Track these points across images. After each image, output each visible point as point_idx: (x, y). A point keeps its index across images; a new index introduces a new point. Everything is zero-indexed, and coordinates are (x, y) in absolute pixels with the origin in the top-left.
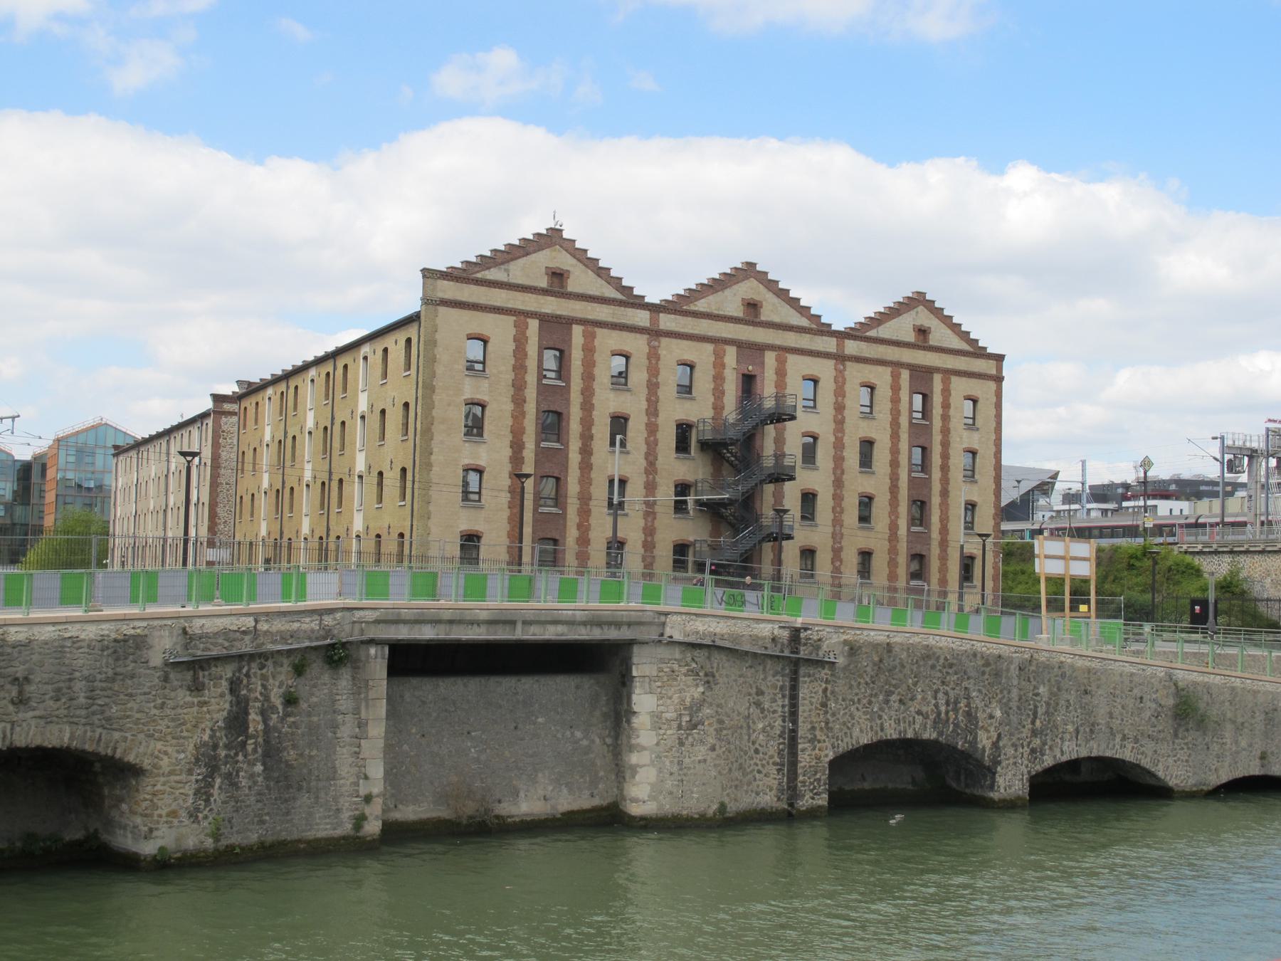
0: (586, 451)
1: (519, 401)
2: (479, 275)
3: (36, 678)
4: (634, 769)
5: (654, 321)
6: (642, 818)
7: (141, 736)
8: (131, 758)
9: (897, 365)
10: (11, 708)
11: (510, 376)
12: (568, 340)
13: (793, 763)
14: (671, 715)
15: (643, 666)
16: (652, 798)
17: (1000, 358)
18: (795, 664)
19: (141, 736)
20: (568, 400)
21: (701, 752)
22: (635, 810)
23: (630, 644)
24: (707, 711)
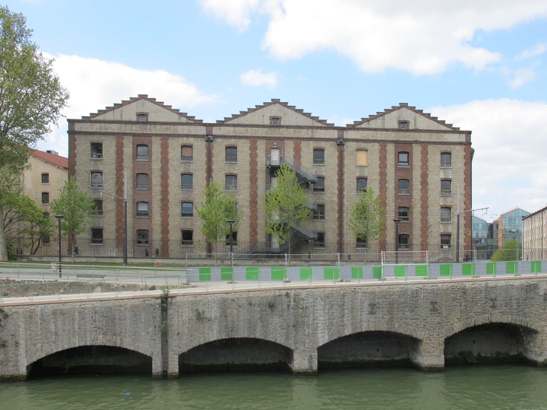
3: (498, 299)
7: (537, 320)
8: (533, 327)
10: (490, 309)
19: (537, 320)
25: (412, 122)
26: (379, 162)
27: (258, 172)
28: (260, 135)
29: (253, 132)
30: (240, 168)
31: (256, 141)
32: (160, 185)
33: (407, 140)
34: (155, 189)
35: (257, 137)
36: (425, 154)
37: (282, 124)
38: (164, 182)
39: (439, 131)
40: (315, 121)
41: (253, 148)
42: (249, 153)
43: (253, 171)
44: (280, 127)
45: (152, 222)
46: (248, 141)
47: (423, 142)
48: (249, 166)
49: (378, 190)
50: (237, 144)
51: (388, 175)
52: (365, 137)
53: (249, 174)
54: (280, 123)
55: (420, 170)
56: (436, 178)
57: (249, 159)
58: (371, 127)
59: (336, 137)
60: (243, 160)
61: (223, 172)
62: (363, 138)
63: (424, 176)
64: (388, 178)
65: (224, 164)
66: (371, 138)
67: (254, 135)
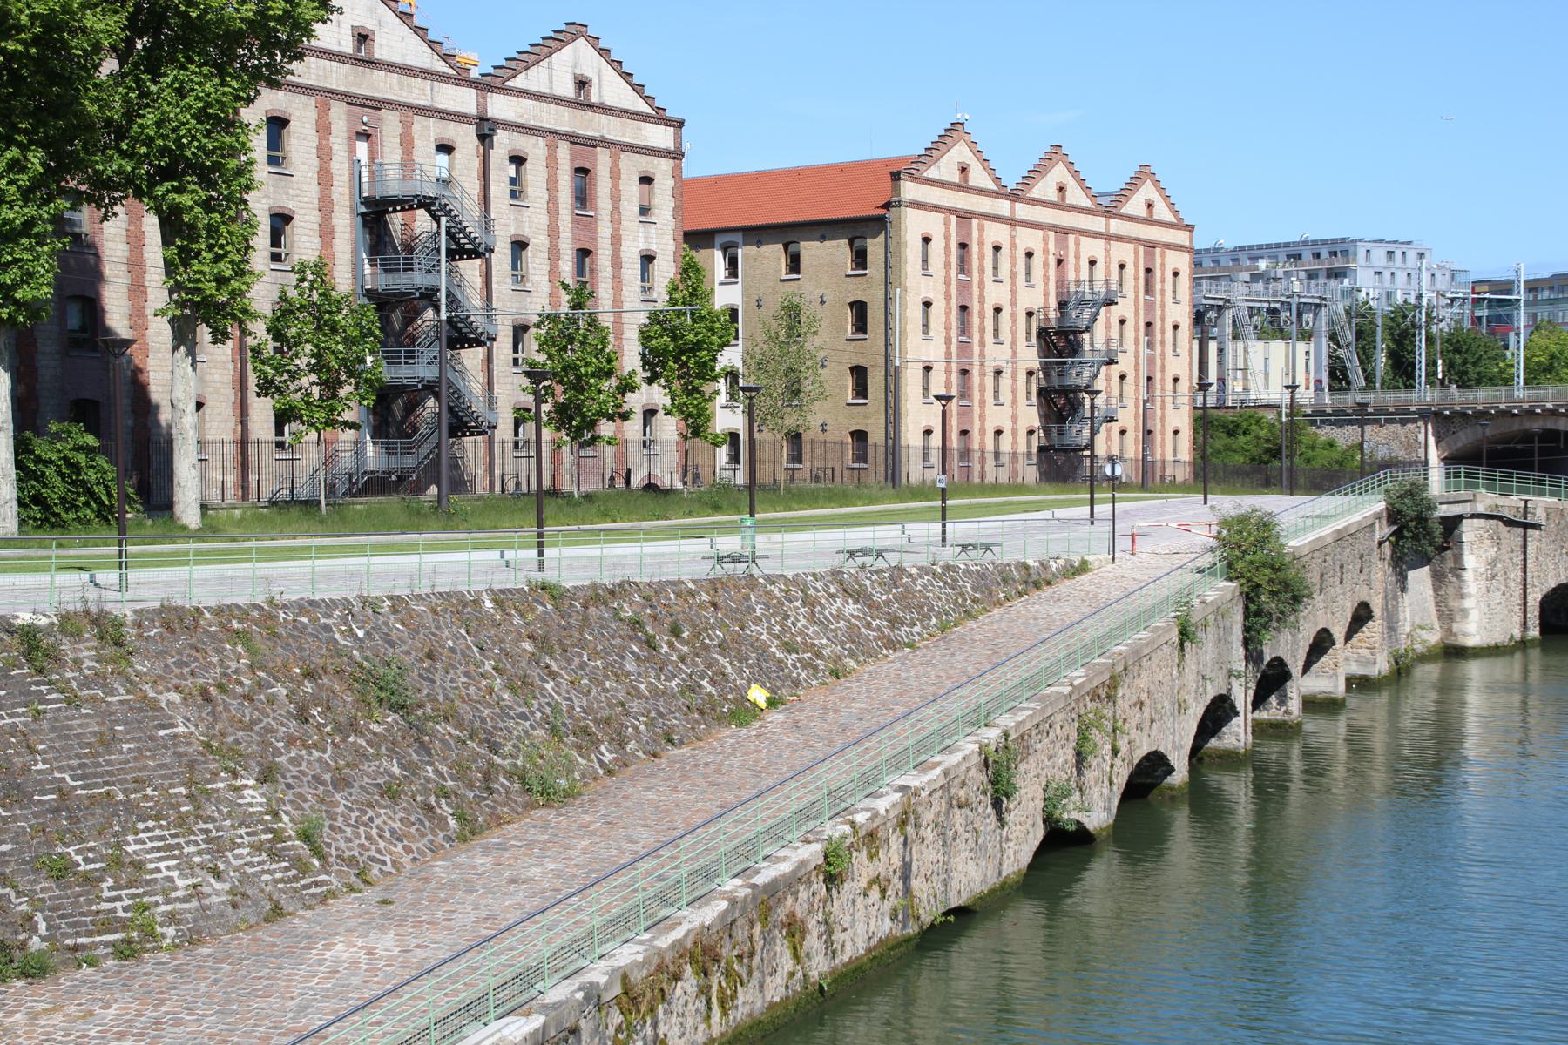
0: (982, 344)
1: (948, 297)
2: (925, 175)
4: (1464, 612)
5: (1013, 210)
6: (1474, 648)
9: (1138, 241)
11: (943, 273)
12: (969, 235)
13: (1525, 604)
14: (1482, 570)
15: (1470, 531)
16: (1478, 633)
17: (1191, 228)
18: (1527, 526)
20: (971, 294)
21: (1498, 596)
22: (1471, 642)
23: (1459, 518)
24: (1499, 566)
25: (595, 81)
26: (546, 196)
27: (336, 208)
28: (334, 87)
29: (321, 73)
30: (297, 192)
31: (328, 104)
32: (124, 239)
33: (589, 133)
34: (112, 253)
35: (331, 92)
36: (615, 175)
37: (378, 54)
38: (132, 228)
39: (637, 114)
40: (436, 57)
41: (323, 129)
42: (315, 145)
43: (326, 206)
44: (372, 63)
45: (108, 370)
46: (312, 101)
47: (613, 143)
48: (317, 188)
49: (547, 278)
50: (290, 110)
51: (561, 235)
52: (522, 116)
53: (317, 213)
54: (370, 51)
55: (609, 224)
56: (634, 250)
57: (316, 162)
58: (534, 88)
59: (473, 111)
60: (304, 164)
61: (264, 201)
62: (520, 121)
63: (616, 241)
64: (561, 246)
65: (265, 174)
66: (532, 123)
67: (322, 84)
